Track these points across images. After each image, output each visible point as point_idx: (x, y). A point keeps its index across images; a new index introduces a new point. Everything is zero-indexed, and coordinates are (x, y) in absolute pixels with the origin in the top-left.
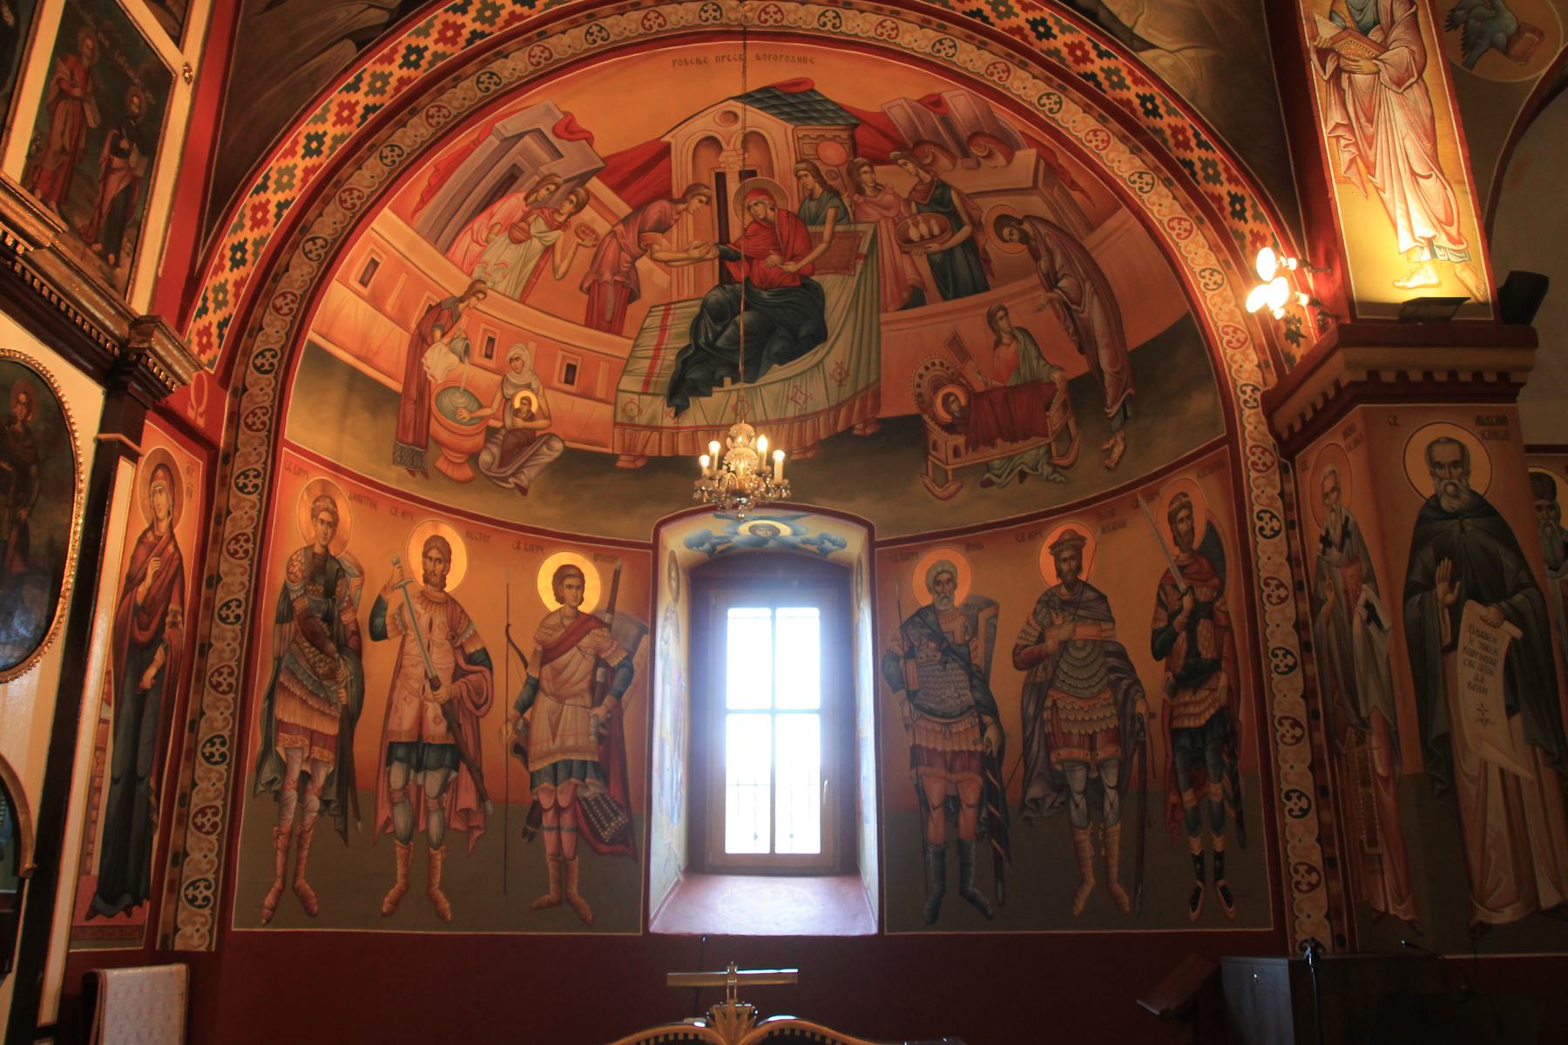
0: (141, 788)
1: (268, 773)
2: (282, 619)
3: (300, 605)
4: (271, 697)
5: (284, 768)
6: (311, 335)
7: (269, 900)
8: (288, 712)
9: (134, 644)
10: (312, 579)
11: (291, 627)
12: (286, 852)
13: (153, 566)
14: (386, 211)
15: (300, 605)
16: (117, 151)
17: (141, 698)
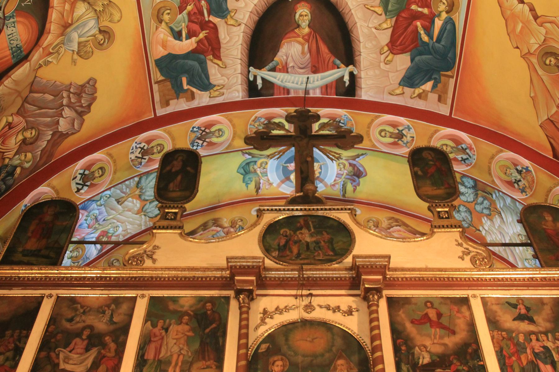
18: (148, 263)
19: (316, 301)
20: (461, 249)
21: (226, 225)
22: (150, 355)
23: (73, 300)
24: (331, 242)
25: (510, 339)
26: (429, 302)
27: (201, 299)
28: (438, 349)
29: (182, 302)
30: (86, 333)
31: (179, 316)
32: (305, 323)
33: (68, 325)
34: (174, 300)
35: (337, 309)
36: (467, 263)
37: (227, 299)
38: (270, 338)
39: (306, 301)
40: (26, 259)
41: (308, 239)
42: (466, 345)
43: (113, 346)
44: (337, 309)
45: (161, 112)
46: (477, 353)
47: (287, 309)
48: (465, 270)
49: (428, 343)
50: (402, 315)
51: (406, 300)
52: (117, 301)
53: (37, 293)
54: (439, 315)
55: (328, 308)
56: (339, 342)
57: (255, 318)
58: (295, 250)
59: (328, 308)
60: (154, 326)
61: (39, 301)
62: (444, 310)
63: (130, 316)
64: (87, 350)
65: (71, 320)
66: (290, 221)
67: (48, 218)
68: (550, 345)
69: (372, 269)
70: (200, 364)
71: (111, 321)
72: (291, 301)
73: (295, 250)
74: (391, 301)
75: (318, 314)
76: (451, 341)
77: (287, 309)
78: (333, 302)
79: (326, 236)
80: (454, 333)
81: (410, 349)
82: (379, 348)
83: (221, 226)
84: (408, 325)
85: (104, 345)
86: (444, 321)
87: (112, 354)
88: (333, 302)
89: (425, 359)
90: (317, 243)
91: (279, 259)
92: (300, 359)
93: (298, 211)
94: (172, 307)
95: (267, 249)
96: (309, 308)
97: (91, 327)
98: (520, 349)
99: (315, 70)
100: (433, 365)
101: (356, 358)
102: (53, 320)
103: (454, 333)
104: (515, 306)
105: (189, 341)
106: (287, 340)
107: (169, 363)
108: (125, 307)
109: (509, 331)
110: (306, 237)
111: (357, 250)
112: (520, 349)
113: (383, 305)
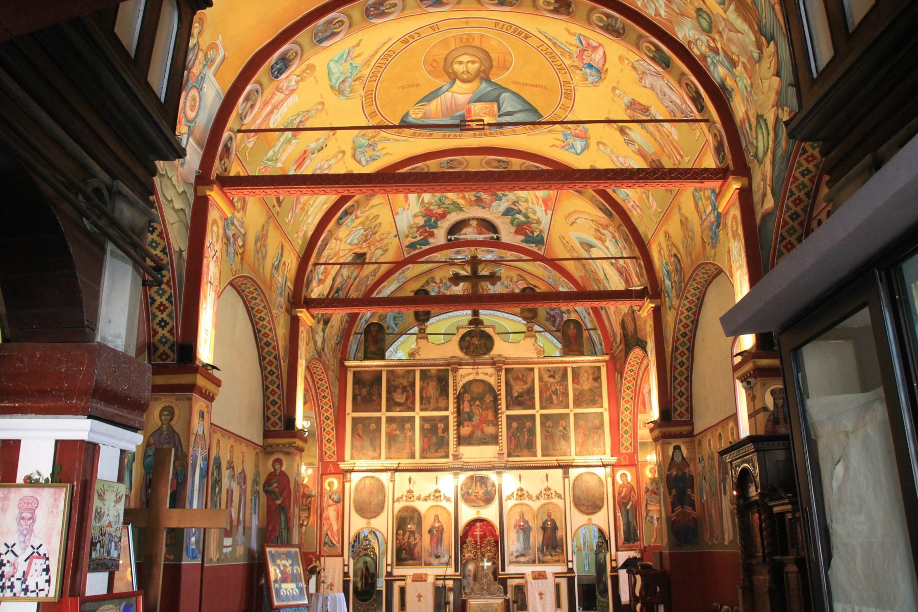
0: (632, 525)
1: (648, 519)
2: (646, 492)
3: (650, 488)
4: (646, 506)
5: (652, 518)
6: (639, 441)
7: (653, 540)
8: (649, 508)
9: (623, 503)
10: (652, 483)
11: (649, 493)
12: (656, 531)
13: (625, 490)
14: (639, 415)
15: (650, 488)
16: (594, 433)
17: (627, 512)
18: (417, 357)
19: (480, 371)
20: (534, 347)
21: (438, 281)
22: (424, 395)
23: (392, 372)
24: (485, 344)
25: (545, 385)
26: (519, 369)
27: (439, 370)
28: (520, 390)
29: (432, 371)
30: (401, 386)
31: (431, 377)
32: (476, 381)
33: (393, 383)
34: (429, 370)
35: (487, 374)
36: (535, 355)
37: (448, 370)
38: (464, 386)
39: (475, 371)
40: (372, 356)
41: (477, 343)
42: (530, 389)
43: (411, 391)
44: (487, 374)
45: (406, 256)
46: (533, 392)
47: (469, 374)
48: (533, 358)
49: (517, 388)
50: (510, 376)
51: (512, 369)
52: (408, 371)
53: (379, 369)
54: (523, 376)
55: (484, 373)
56: (487, 388)
57: (458, 378)
58: (472, 349)
59: (484, 373)
60: (424, 382)
61: (381, 372)
62: (525, 373)
63: (414, 378)
64: (403, 393)
65: (394, 381)
66: (468, 334)
67: (374, 334)
68: (558, 388)
69: (500, 362)
70: (441, 398)
71: (408, 381)
72: (470, 371)
73: (472, 349)
74: (506, 369)
75: (481, 377)
76: (525, 387)
77: (469, 374)
78: (486, 371)
79: (484, 341)
80: (526, 383)
81: (511, 390)
82: (500, 394)
83: (435, 282)
84: (512, 381)
85: (408, 392)
86: (524, 378)
87: (411, 395)
88: (486, 371)
89: (516, 394)
90: (480, 345)
91: (466, 353)
92: (474, 395)
93: (472, 327)
94: (429, 374)
95: (462, 348)
96: (477, 373)
97: (401, 384)
98: (548, 389)
99: (479, 234)
100: (517, 397)
101: (493, 394)
102: (388, 381)
103: (526, 383)
104: (550, 371)
105: (436, 388)
106: (470, 386)
107: (430, 398)
108: (412, 375)
109: (545, 382)
110: (476, 341)
111: (494, 352)
112: (548, 389)
113: (503, 372)
